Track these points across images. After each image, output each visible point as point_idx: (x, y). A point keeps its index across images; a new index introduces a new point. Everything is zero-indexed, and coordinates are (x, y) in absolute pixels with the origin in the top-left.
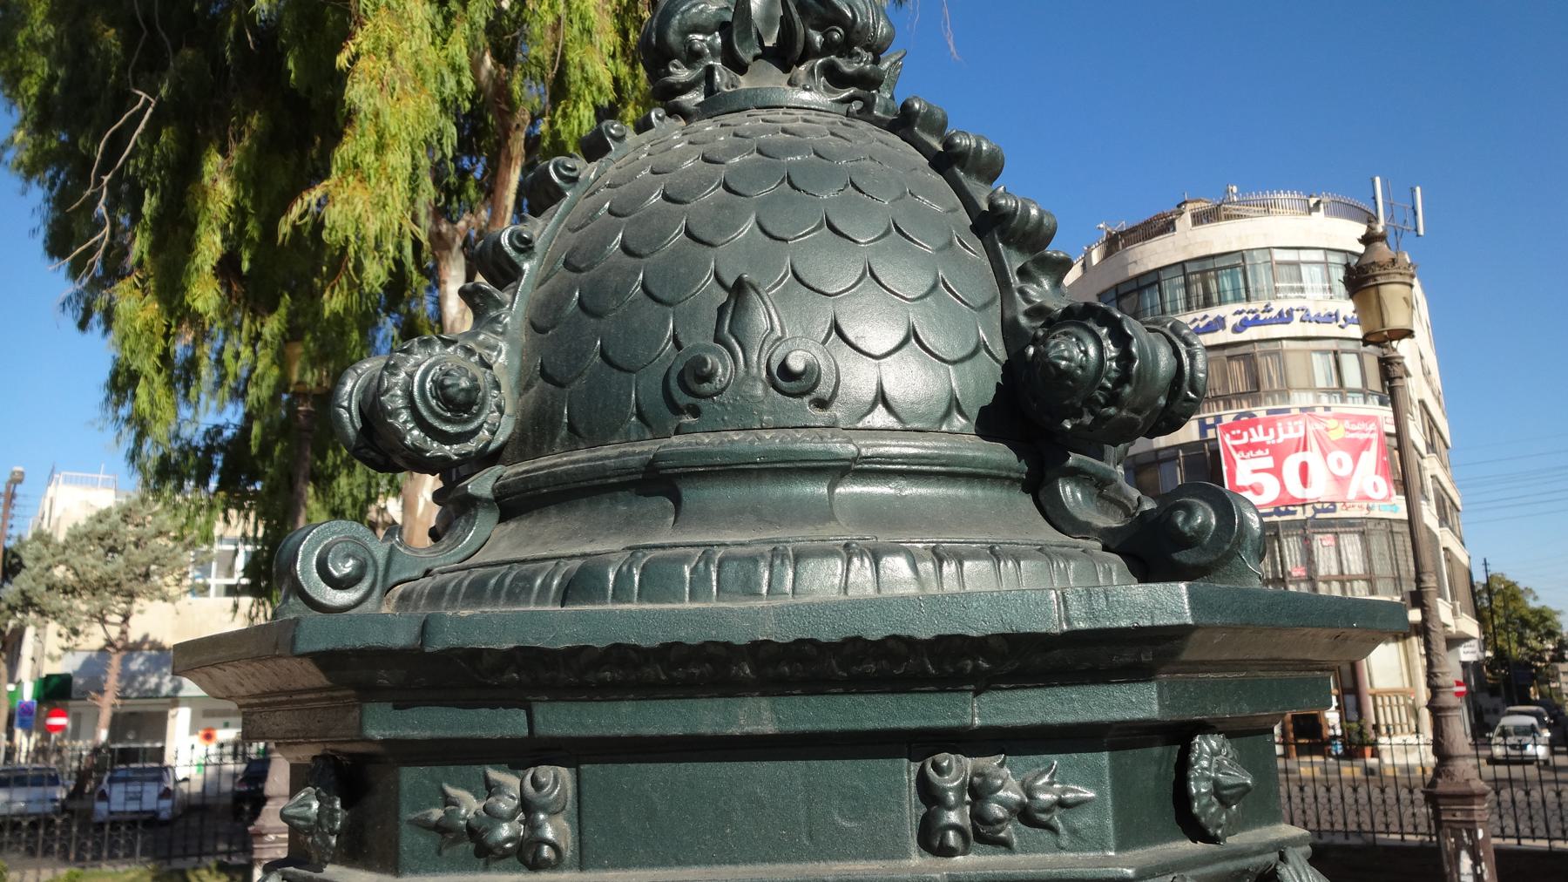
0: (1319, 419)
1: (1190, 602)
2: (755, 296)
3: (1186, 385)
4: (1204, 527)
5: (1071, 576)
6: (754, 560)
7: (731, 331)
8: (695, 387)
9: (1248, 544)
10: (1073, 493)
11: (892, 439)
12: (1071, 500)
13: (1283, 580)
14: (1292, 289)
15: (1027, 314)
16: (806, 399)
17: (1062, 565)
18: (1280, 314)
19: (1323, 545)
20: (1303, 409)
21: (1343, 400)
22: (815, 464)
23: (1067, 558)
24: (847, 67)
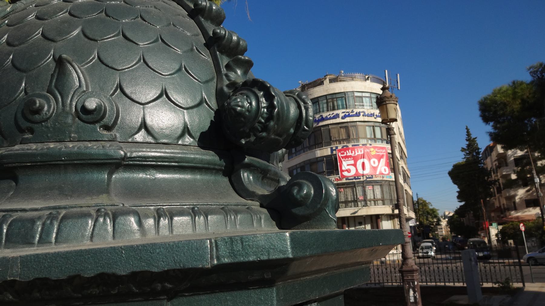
0: (368, 148)
1: (291, 244)
2: (69, 66)
3: (303, 123)
4: (308, 194)
5: (238, 222)
6: (33, 221)
7: (56, 87)
8: (30, 117)
9: (330, 204)
10: (248, 178)
11: (147, 148)
12: (246, 180)
14: (360, 105)
15: (228, 86)
16: (98, 126)
17: (233, 217)
18: (356, 113)
19: (369, 189)
20: (363, 145)
22: (98, 161)
23: (236, 212)
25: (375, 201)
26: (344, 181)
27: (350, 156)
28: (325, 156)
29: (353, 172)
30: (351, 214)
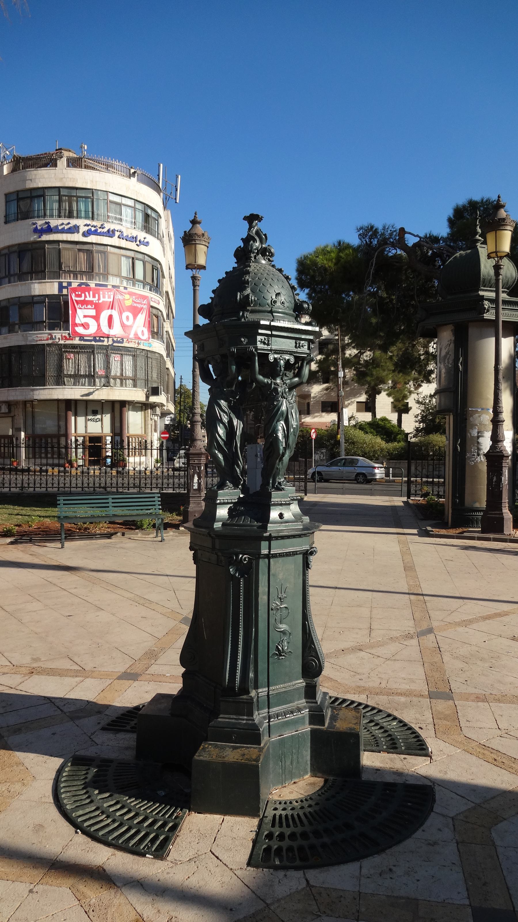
0: (121, 293)
13: (93, 376)
14: (116, 218)
19: (115, 359)
20: (114, 286)
21: (134, 285)
24: (271, 259)
25: (123, 379)
26: (77, 341)
27: (91, 303)
28: (47, 296)
29: (93, 329)
30: (82, 396)
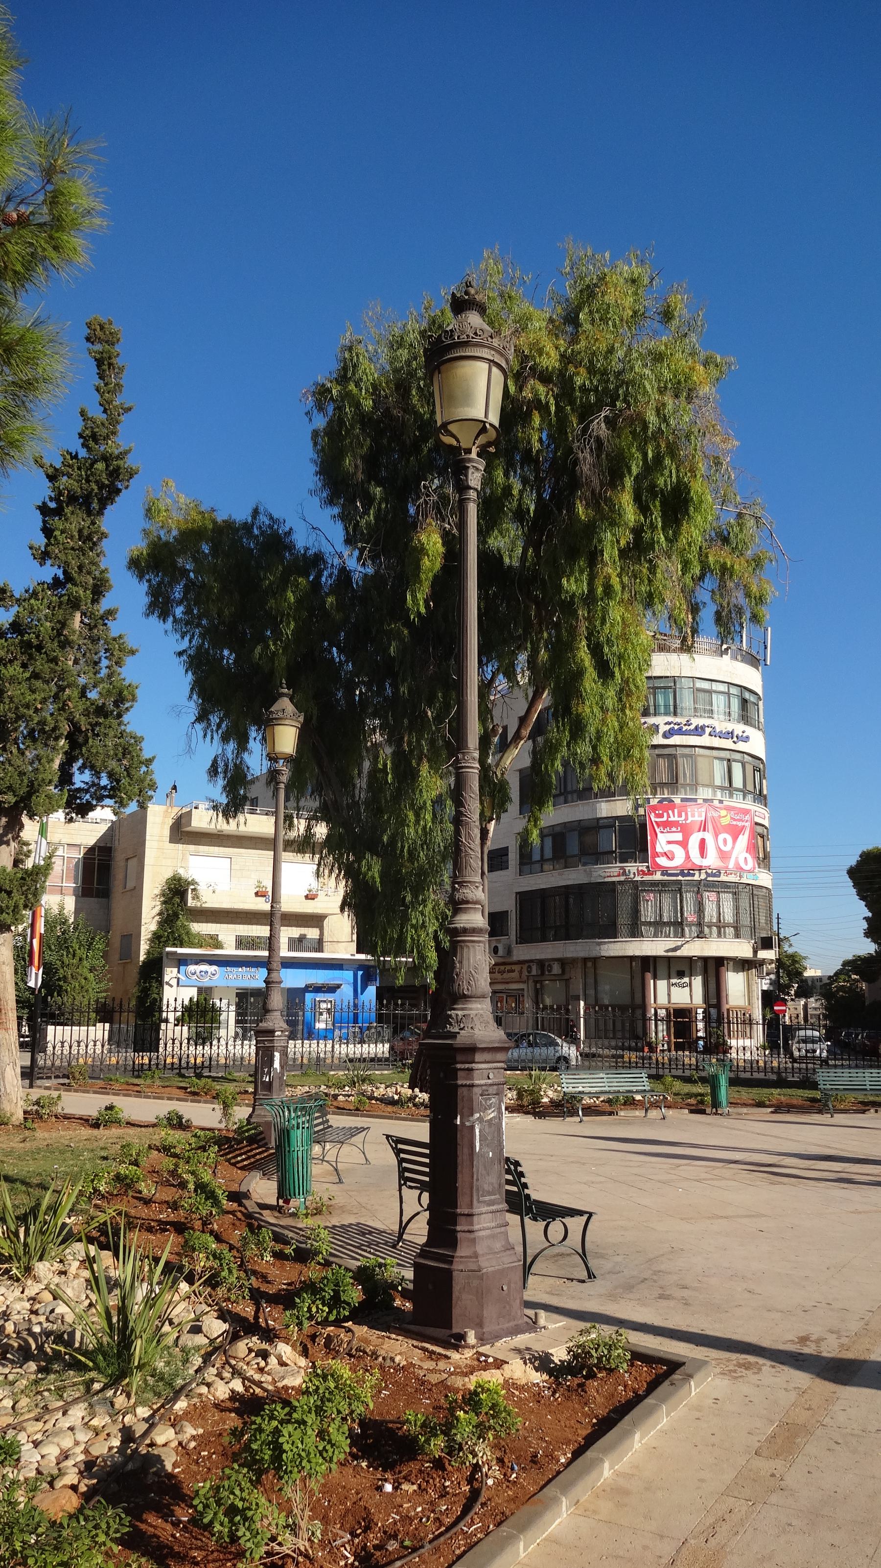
0: (715, 809)
13: (681, 924)
14: (705, 710)
18: (696, 728)
19: (709, 899)
20: (705, 800)
21: (731, 796)
25: (720, 926)
26: (658, 876)
27: (675, 824)
28: (617, 818)
29: (679, 860)
30: (667, 951)
